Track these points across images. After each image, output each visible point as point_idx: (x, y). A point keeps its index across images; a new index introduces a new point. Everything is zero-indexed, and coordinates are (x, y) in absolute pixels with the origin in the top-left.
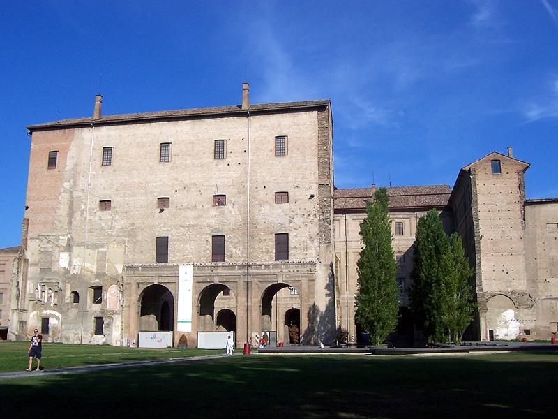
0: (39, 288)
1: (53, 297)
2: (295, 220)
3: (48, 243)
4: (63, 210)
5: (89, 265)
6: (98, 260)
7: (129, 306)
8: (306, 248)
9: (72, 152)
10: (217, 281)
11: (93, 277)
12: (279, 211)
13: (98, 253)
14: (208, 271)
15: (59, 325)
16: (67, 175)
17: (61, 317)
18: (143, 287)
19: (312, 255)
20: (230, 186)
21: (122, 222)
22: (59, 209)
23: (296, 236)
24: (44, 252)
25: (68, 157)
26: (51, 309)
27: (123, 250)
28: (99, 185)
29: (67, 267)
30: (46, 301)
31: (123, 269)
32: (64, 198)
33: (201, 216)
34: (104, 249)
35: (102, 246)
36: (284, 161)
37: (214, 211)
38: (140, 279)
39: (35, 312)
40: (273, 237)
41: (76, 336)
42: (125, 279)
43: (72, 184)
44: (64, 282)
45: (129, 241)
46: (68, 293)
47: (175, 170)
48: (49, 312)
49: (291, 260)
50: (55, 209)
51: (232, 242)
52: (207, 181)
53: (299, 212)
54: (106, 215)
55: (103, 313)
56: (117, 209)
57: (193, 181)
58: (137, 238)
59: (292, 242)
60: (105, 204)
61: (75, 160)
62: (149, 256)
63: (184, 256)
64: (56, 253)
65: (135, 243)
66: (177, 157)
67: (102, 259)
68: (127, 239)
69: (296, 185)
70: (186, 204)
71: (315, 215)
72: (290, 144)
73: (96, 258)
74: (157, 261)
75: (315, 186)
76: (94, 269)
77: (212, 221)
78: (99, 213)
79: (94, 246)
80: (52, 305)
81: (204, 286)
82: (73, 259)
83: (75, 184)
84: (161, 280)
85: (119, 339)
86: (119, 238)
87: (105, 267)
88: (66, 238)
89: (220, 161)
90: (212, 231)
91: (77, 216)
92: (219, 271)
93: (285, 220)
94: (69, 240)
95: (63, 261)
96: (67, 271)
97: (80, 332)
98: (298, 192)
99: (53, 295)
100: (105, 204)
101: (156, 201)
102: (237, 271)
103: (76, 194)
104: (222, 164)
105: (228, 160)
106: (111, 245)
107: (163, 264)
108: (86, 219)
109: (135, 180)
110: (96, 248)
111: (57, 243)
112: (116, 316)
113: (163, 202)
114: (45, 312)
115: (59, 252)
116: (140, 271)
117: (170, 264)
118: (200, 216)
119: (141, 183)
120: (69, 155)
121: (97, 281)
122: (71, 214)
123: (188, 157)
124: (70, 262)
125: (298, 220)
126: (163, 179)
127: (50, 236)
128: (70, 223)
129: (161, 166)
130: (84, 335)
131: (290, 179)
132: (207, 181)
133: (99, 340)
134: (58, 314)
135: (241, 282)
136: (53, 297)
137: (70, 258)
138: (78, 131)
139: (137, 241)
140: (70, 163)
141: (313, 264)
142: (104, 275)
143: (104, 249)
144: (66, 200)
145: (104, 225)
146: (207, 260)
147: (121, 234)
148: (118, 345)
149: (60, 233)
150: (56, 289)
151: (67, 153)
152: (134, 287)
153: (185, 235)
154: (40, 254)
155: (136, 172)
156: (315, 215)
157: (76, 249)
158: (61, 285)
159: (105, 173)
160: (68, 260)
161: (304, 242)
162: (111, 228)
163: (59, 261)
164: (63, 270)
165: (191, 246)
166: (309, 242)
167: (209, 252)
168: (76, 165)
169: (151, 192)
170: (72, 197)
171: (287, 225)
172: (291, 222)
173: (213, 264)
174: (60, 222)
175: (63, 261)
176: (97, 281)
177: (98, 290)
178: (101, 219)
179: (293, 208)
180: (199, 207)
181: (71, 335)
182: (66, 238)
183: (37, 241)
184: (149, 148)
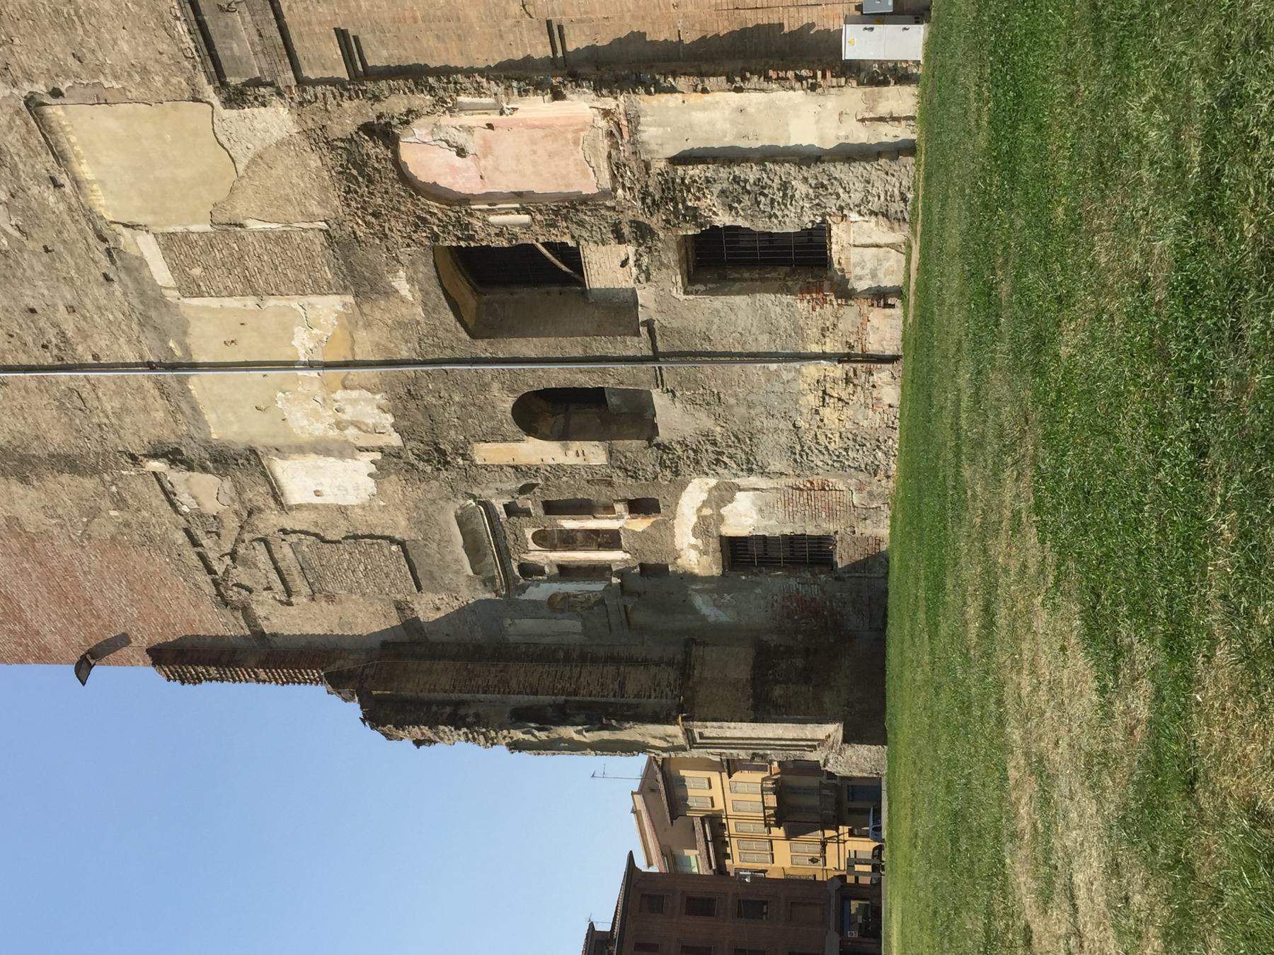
3: (249, 564)
6: (250, 288)
7: (554, 31)
11: (380, 312)
13: (191, 288)
26: (667, 526)
29: (364, 464)
34: (148, 248)
41: (839, 391)
46: (537, 451)
73: (228, 302)
80: (640, 524)
87: (281, 239)
88: (175, 476)
97: (812, 371)
111: (232, 523)
112: (649, 133)
121: (401, 284)
127: (202, 557)
133: (867, 247)
137: (301, 449)
142: (340, 244)
154: (330, 598)
160: (312, 459)
163: (342, 510)
164: (394, 485)
174: (94, 513)
175: (330, 483)
176: (401, 284)
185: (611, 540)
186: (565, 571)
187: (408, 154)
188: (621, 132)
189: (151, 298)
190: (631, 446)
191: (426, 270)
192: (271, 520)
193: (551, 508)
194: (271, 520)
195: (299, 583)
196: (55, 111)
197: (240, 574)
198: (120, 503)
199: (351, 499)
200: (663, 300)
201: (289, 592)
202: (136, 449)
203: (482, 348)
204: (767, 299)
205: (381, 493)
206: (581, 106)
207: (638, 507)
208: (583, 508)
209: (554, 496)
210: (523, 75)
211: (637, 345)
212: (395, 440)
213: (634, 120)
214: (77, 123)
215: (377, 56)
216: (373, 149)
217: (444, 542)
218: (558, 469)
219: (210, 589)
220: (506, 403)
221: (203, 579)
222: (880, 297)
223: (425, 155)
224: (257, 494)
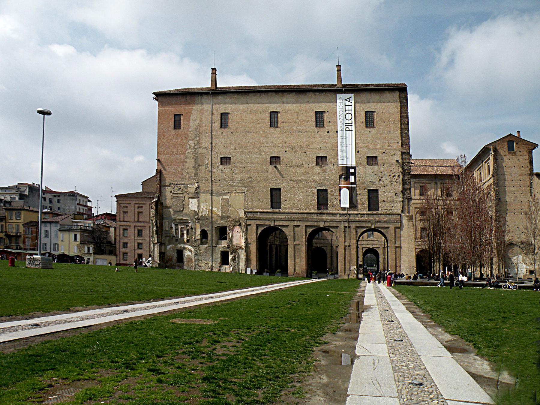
0: (173, 226)
1: (185, 235)
2: (383, 179)
4: (190, 163)
6: (222, 206)
8: (392, 202)
10: (322, 225)
11: (219, 219)
12: (371, 171)
14: (315, 217)
16: (191, 134)
17: (193, 250)
18: (260, 229)
20: (330, 150)
21: (242, 175)
22: (186, 162)
23: (384, 192)
24: (175, 196)
25: (191, 120)
27: (242, 198)
28: (220, 144)
29: (196, 210)
30: (180, 237)
31: (245, 212)
32: (190, 153)
33: (308, 173)
35: (225, 194)
37: (317, 169)
38: (258, 222)
39: (171, 246)
43: (196, 142)
44: (194, 222)
45: (247, 191)
46: (198, 231)
47: (284, 134)
48: (182, 246)
51: (333, 195)
52: (311, 144)
53: (386, 173)
54: (226, 168)
55: (228, 248)
56: (236, 164)
57: (299, 144)
58: (255, 189)
60: (225, 160)
61: (198, 122)
62: (265, 204)
63: (294, 204)
64: (186, 199)
65: (253, 192)
66: (284, 125)
67: (226, 204)
68: (246, 189)
69: (383, 151)
70: (294, 163)
71: (399, 176)
74: (272, 207)
76: (220, 214)
77: (317, 177)
78: (221, 167)
79: (219, 194)
80: (185, 240)
82: (201, 204)
83: (199, 142)
84: (277, 223)
85: (244, 269)
86: (240, 188)
87: (228, 211)
89: (322, 129)
90: (317, 185)
91: (202, 168)
92: (324, 217)
93: (376, 179)
95: (193, 205)
96: (196, 213)
97: (210, 262)
98: (385, 157)
99: (185, 232)
100: (225, 160)
101: (269, 159)
107: (277, 210)
109: (251, 141)
110: (221, 195)
111: (186, 190)
113: (275, 160)
115: (189, 198)
119: (255, 144)
120: (192, 118)
121: (222, 222)
122: (197, 167)
123: (294, 125)
124: (199, 206)
126: (274, 142)
128: (196, 174)
130: (214, 265)
131: (378, 146)
132: (311, 144)
133: (227, 269)
134: (190, 247)
135: (342, 226)
136: (185, 235)
137: (199, 203)
138: (198, 98)
139: (255, 191)
140: (193, 125)
143: (227, 197)
144: (191, 155)
145: (226, 177)
146: (313, 209)
147: (241, 185)
150: (188, 228)
151: (190, 116)
153: (294, 188)
155: (251, 135)
156: (399, 176)
157: (202, 195)
159: (224, 134)
160: (197, 204)
161: (391, 196)
163: (188, 205)
165: (300, 197)
166: (395, 197)
167: (315, 202)
168: (200, 126)
169: (264, 152)
171: (377, 183)
172: (380, 180)
173: (320, 211)
174: (188, 173)
175: (193, 205)
179: (382, 169)
182: (194, 186)
183: (169, 188)
184: (260, 115)
186: (177, 229)
187: (238, 227)
189: (221, 194)
190: (199, 242)
191: (224, 225)
192: (187, 196)
193: (188, 231)
194: (187, 196)
195: (174, 195)
196: (243, 194)
198: (189, 177)
199: (190, 207)
200: (220, 248)
201: (173, 193)
202: (199, 184)
203: (214, 228)
204: (220, 259)
205: (191, 211)
206: (243, 245)
207: (188, 241)
208: (187, 234)
209: (190, 231)
210: (246, 239)
211: (214, 245)
212: (200, 215)
213: (243, 249)
214: (242, 196)
215: (249, 227)
216: (238, 223)
217: (183, 216)
218: (195, 233)
219: (174, 183)
220: (206, 229)
221: (176, 183)
222: (220, 270)
223: (237, 228)
224: (190, 195)
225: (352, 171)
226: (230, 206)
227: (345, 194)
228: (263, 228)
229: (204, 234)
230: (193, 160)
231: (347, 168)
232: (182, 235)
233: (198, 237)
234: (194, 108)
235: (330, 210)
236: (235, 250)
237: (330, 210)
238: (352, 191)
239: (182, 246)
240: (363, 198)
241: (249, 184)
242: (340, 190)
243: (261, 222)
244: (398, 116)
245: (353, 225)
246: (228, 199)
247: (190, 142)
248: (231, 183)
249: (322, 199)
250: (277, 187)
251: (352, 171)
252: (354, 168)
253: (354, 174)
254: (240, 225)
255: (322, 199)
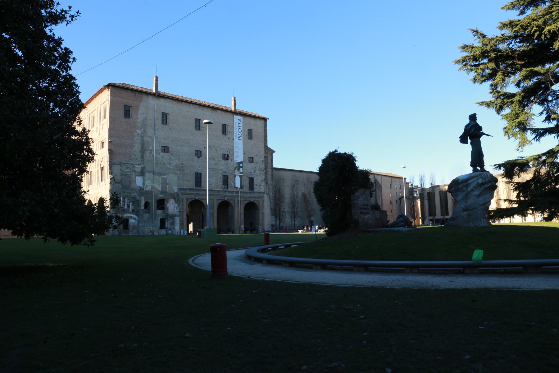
2: (256, 172)
4: (137, 148)
5: (156, 186)
6: (162, 183)
8: (260, 186)
9: (142, 110)
13: (162, 178)
15: (136, 223)
19: (262, 190)
26: (130, 213)
29: (142, 186)
30: (126, 207)
32: (137, 139)
35: (164, 175)
36: (252, 142)
37: (223, 162)
38: (188, 196)
40: (248, 179)
42: (180, 195)
44: (140, 196)
46: (143, 203)
48: (128, 215)
49: (255, 190)
50: (132, 146)
54: (165, 155)
59: (255, 182)
60: (165, 149)
62: (191, 184)
67: (164, 183)
68: (179, 172)
72: (254, 134)
74: (196, 186)
75: (263, 157)
76: (160, 189)
77: (223, 167)
78: (162, 154)
79: (160, 174)
80: (131, 210)
81: (220, 201)
83: (145, 132)
88: (140, 166)
89: (225, 136)
91: (147, 153)
92: (227, 194)
93: (252, 171)
94: (143, 169)
95: (139, 181)
96: (141, 189)
100: (165, 149)
101: (194, 152)
102: (234, 194)
103: (146, 139)
104: (226, 138)
105: (229, 136)
106: (170, 175)
108: (153, 156)
114: (125, 215)
115: (136, 176)
116: (188, 192)
117: (202, 188)
118: (217, 164)
120: (140, 111)
121: (162, 196)
122: (143, 151)
124: (144, 184)
125: (258, 172)
128: (142, 157)
129: (197, 132)
134: (134, 216)
138: (145, 97)
140: (140, 118)
141: (263, 193)
147: (175, 168)
148: (179, 234)
149: (135, 163)
151: (138, 110)
152: (185, 201)
157: (147, 174)
158: (138, 198)
162: (170, 164)
163: (135, 181)
170: (144, 140)
175: (139, 181)
176: (162, 196)
177: (161, 204)
178: (163, 158)
180: (216, 159)
181: (146, 230)
182: (140, 166)
183: (119, 166)
185: (128, 206)
188: (176, 216)
193: (133, 202)
194: (134, 174)
197: (125, 167)
198: (136, 159)
199: (137, 183)
207: (133, 210)
220: (149, 201)
225: (241, 165)
226: (168, 184)
227: (238, 179)
228: (190, 200)
229: (147, 205)
230: (140, 146)
231: (239, 163)
232: (128, 206)
233: (143, 208)
234: (142, 104)
235: (230, 189)
236: (173, 216)
237: (230, 189)
238: (241, 177)
239: (128, 215)
240: (246, 183)
241: (181, 168)
242: (235, 177)
243: (190, 196)
244: (263, 136)
245: (242, 199)
246: (166, 179)
247: (138, 131)
248: (169, 166)
249: (226, 181)
250: (199, 172)
251: (241, 165)
252: (242, 163)
253: (242, 167)
254: (174, 198)
255: (226, 181)
